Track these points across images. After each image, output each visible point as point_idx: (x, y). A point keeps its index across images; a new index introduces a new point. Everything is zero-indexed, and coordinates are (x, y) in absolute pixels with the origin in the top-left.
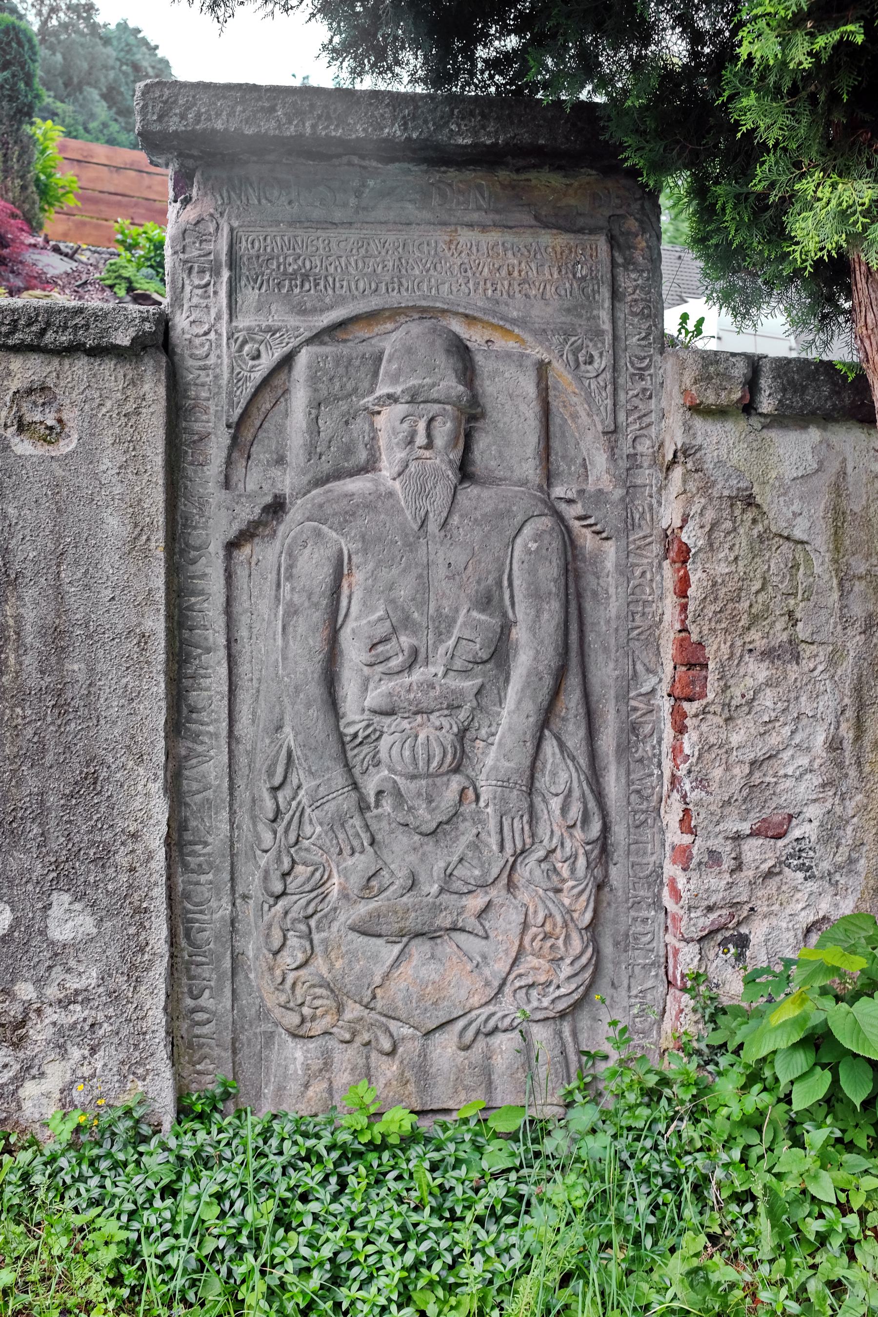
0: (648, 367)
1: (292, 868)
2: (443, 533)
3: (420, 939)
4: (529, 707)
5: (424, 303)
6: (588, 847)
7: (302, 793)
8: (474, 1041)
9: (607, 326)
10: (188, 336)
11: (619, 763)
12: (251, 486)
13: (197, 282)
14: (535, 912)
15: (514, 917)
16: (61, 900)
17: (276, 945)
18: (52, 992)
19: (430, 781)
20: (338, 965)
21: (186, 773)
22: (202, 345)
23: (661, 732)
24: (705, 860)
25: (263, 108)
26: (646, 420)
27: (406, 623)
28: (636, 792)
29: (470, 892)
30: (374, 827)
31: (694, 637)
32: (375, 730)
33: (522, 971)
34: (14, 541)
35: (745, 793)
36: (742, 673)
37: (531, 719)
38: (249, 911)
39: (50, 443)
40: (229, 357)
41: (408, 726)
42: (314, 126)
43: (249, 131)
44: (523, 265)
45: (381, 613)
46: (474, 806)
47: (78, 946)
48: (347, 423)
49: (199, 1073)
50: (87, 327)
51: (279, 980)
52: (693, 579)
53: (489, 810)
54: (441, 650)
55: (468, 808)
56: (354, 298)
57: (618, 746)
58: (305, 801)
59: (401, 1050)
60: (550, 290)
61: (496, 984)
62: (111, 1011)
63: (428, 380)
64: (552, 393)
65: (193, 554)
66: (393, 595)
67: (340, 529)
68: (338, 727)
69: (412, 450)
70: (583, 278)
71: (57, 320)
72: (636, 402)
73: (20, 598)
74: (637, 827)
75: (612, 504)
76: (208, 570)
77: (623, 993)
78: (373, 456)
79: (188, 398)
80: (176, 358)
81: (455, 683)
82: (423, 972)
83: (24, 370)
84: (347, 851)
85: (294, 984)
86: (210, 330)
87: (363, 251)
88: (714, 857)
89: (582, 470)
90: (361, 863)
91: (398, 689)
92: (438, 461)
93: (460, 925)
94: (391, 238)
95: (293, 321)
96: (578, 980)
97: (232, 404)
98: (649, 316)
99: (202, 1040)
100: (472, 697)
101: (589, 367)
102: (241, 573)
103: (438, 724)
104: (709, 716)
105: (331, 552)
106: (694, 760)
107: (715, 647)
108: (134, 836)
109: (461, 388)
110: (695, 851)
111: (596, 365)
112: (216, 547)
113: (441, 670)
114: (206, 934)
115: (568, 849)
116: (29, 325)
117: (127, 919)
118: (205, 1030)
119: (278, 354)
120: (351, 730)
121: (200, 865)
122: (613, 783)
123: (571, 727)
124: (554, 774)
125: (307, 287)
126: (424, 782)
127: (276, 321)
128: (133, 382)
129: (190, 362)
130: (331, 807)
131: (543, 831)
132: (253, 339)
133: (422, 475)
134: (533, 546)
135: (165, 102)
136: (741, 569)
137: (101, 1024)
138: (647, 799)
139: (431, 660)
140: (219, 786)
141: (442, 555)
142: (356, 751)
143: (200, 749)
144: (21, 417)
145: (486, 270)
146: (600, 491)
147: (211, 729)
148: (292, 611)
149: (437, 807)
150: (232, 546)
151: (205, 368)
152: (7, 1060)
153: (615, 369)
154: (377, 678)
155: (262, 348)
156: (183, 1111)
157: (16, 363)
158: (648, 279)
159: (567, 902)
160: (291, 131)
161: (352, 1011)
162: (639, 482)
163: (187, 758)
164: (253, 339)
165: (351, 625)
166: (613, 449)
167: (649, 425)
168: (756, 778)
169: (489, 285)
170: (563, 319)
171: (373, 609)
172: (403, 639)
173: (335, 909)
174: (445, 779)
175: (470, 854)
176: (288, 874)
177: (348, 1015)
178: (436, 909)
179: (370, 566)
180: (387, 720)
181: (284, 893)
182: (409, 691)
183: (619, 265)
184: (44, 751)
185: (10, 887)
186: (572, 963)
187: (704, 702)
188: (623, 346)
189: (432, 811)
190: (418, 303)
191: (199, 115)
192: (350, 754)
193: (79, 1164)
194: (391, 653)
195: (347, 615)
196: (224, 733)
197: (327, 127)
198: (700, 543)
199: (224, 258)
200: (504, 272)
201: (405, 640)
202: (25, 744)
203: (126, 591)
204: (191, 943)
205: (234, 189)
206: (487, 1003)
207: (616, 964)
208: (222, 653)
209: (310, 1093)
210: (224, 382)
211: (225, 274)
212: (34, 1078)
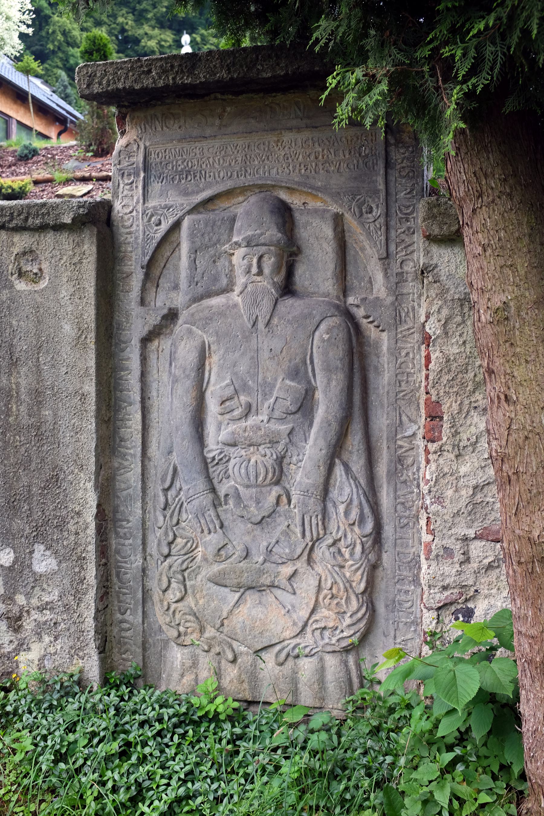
0: (412, 212)
1: (174, 539)
2: (267, 330)
3: (252, 591)
4: (322, 443)
5: (260, 182)
6: (364, 539)
7: (182, 493)
8: (286, 660)
9: (382, 187)
10: (121, 215)
11: (389, 483)
12: (159, 304)
13: (126, 181)
14: (326, 580)
15: (312, 581)
16: (39, 548)
17: (164, 586)
18: (34, 602)
19: (258, 489)
20: (201, 602)
21: (118, 478)
22: (129, 219)
23: (420, 463)
24: (441, 553)
25: (143, 71)
26: (411, 249)
27: (245, 388)
28: (400, 503)
29: (283, 563)
30: (223, 517)
31: (434, 398)
32: (225, 456)
33: (317, 618)
34: (15, 340)
35: (469, 508)
36: (468, 423)
37: (323, 452)
38: (151, 563)
39: (36, 283)
40: (143, 226)
41: (244, 454)
42: (174, 79)
43: (137, 87)
44: (325, 152)
45: (228, 381)
46: (287, 507)
47: (49, 576)
48: (214, 262)
49: (124, 659)
50: (48, 213)
51: (166, 608)
52: (433, 357)
53: (296, 510)
54: (266, 405)
55: (283, 507)
56: (217, 182)
57: (388, 472)
58: (183, 498)
59: (239, 660)
60: (344, 166)
61: (300, 624)
62: (65, 616)
63: (258, 232)
64: (347, 235)
65: (123, 345)
66: (236, 369)
67: (203, 328)
68: (203, 452)
69: (249, 277)
70: (367, 156)
71: (33, 211)
72: (403, 236)
73: (18, 373)
74: (402, 528)
75: (385, 307)
76: (131, 356)
77: (391, 640)
78: (231, 282)
79: (120, 251)
80: (114, 228)
81: (275, 426)
82: (254, 612)
83: (21, 242)
84: (206, 531)
85: (174, 612)
86: (133, 210)
87: (223, 152)
88: (448, 552)
89: (368, 285)
90: (214, 539)
91: (238, 430)
92: (265, 283)
93: (276, 584)
94: (240, 143)
95: (180, 200)
96: (356, 628)
97: (144, 254)
98: (413, 177)
99: (126, 640)
100: (286, 436)
101: (370, 215)
102: (153, 357)
103: (263, 452)
104: (445, 453)
105: (197, 343)
106: (432, 483)
107: (448, 405)
108: (78, 514)
109: (280, 235)
110: (433, 547)
111: (374, 214)
112: (135, 343)
113: (266, 418)
114: (128, 576)
115: (349, 540)
116: (19, 215)
117: (74, 563)
118: (128, 634)
119: (171, 221)
120: (211, 455)
121: (125, 534)
122: (385, 497)
123: (355, 458)
124: (341, 489)
125: (189, 178)
126: (254, 490)
127: (172, 200)
128: (78, 245)
129: (123, 230)
130: (196, 503)
131: (332, 526)
132: (156, 214)
133: (253, 293)
134: (326, 337)
135: (90, 76)
136: (468, 350)
137: (60, 623)
138: (409, 508)
139: (260, 411)
140: (136, 487)
141: (266, 343)
142: (214, 468)
143: (126, 463)
144: (20, 269)
145: (301, 157)
146: (377, 298)
147: (132, 451)
148: (175, 381)
149: (262, 506)
150: (146, 341)
151: (130, 233)
152: (12, 638)
153: (387, 215)
154: (226, 422)
155: (162, 219)
156: (105, 681)
157: (16, 238)
158: (413, 152)
159: (348, 575)
160: (161, 84)
161: (210, 632)
162: (405, 291)
163: (118, 469)
164: (156, 214)
165: (211, 389)
166: (386, 270)
167: (413, 252)
168: (479, 498)
169: (302, 166)
170: (352, 184)
171: (224, 379)
172: (242, 398)
173: (199, 567)
174: (269, 488)
175: (283, 538)
176: (172, 542)
177: (207, 635)
178: (261, 572)
179: (222, 352)
180: (232, 450)
181: (169, 555)
182: (245, 431)
183: (391, 145)
184: (30, 461)
185: (13, 539)
186: (351, 616)
187: (440, 443)
188: (394, 199)
189: (259, 509)
190: (256, 183)
191: (108, 81)
192: (211, 470)
193: (31, 702)
194: (234, 407)
195: (208, 383)
196: (139, 454)
197: (182, 78)
198: (438, 332)
199: (141, 165)
200: (312, 157)
201: (243, 399)
202: (21, 457)
203: (76, 368)
204: (120, 580)
205: (148, 123)
206: (294, 637)
207: (387, 620)
208: (138, 406)
209: (184, 680)
210: (140, 241)
211: (142, 175)
212: (25, 650)
